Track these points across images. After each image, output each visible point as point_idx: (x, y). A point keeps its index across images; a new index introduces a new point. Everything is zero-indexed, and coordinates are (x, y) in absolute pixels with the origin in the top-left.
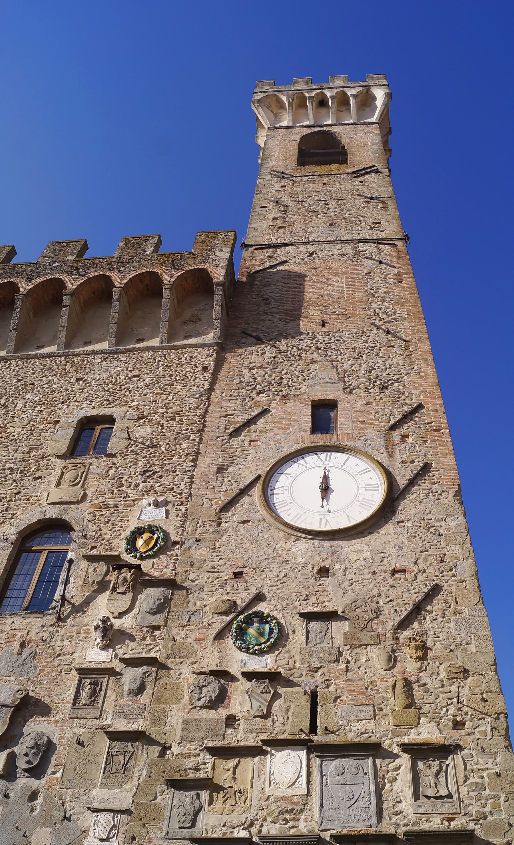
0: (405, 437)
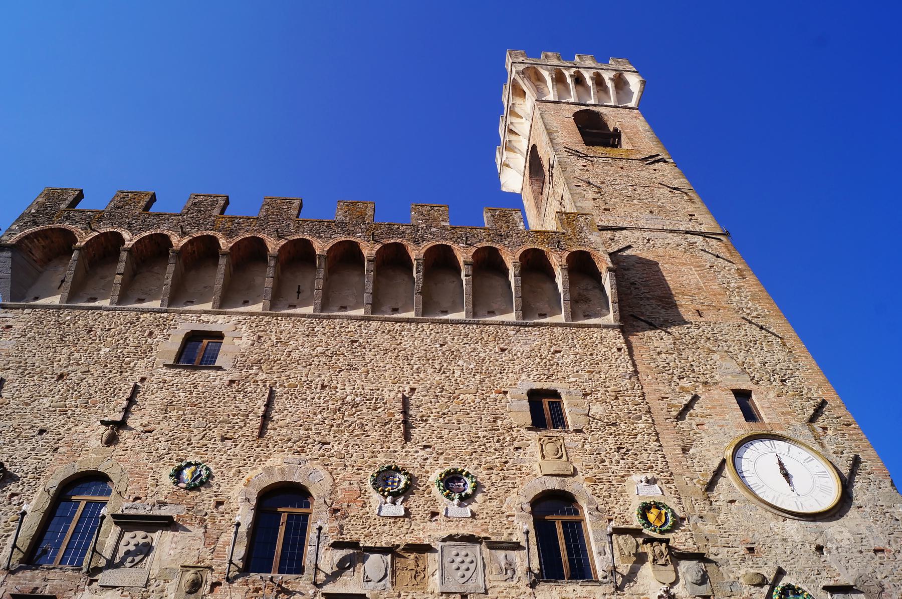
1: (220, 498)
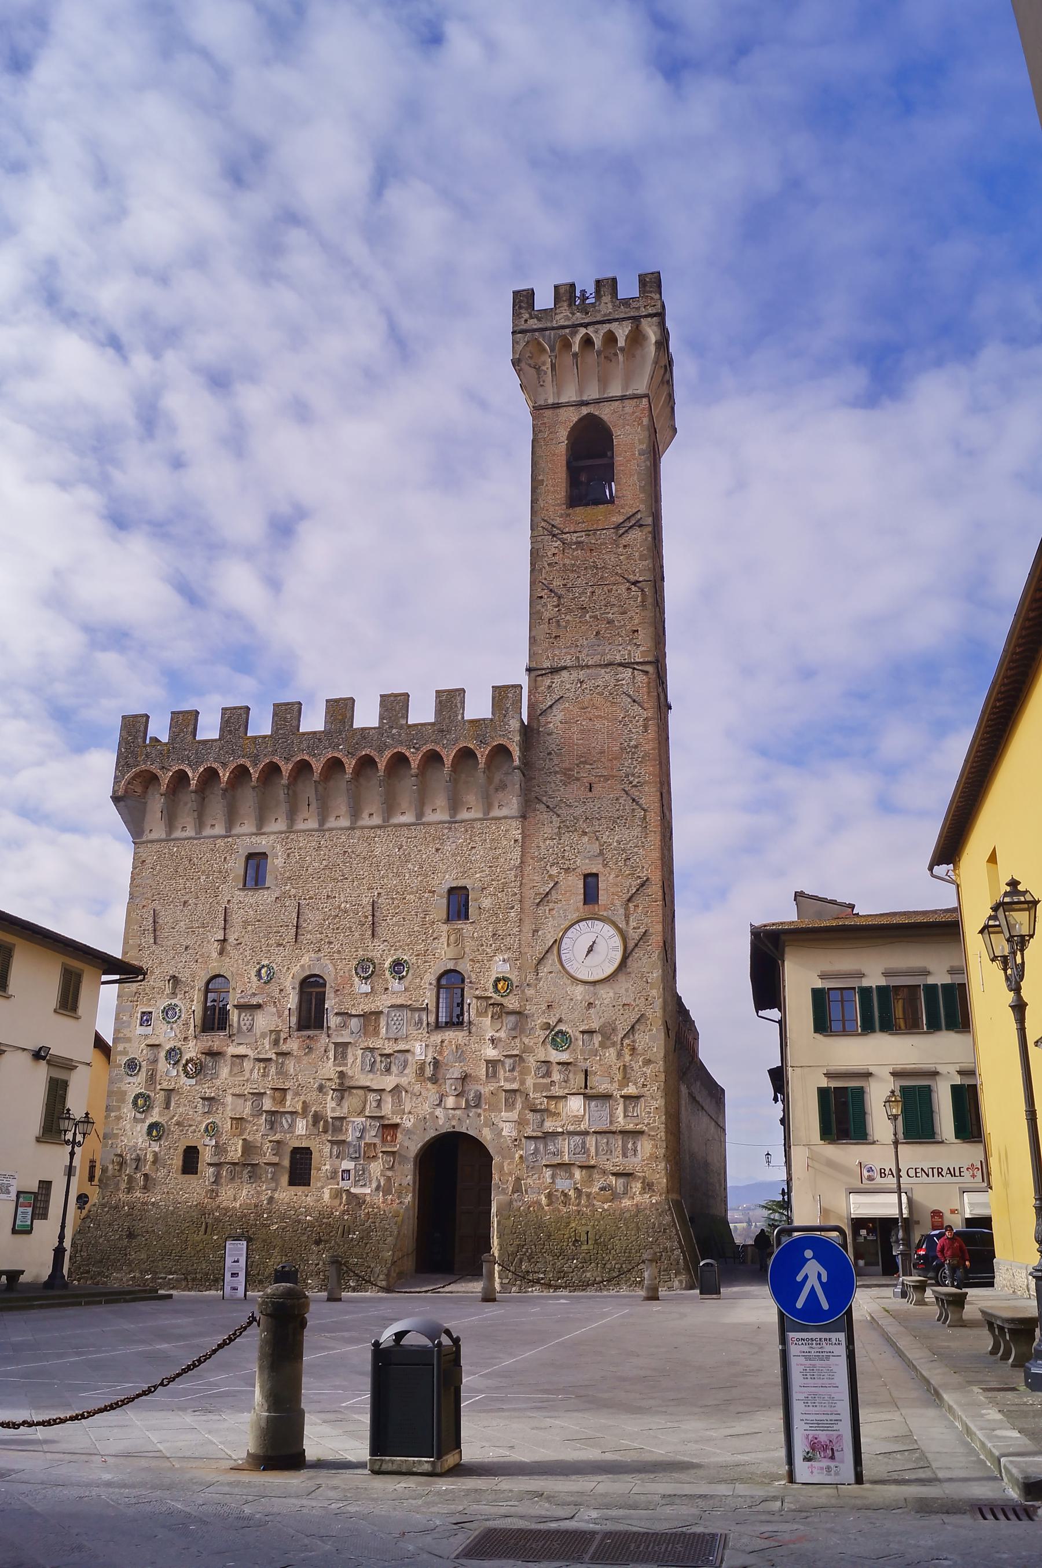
0: (637, 906)
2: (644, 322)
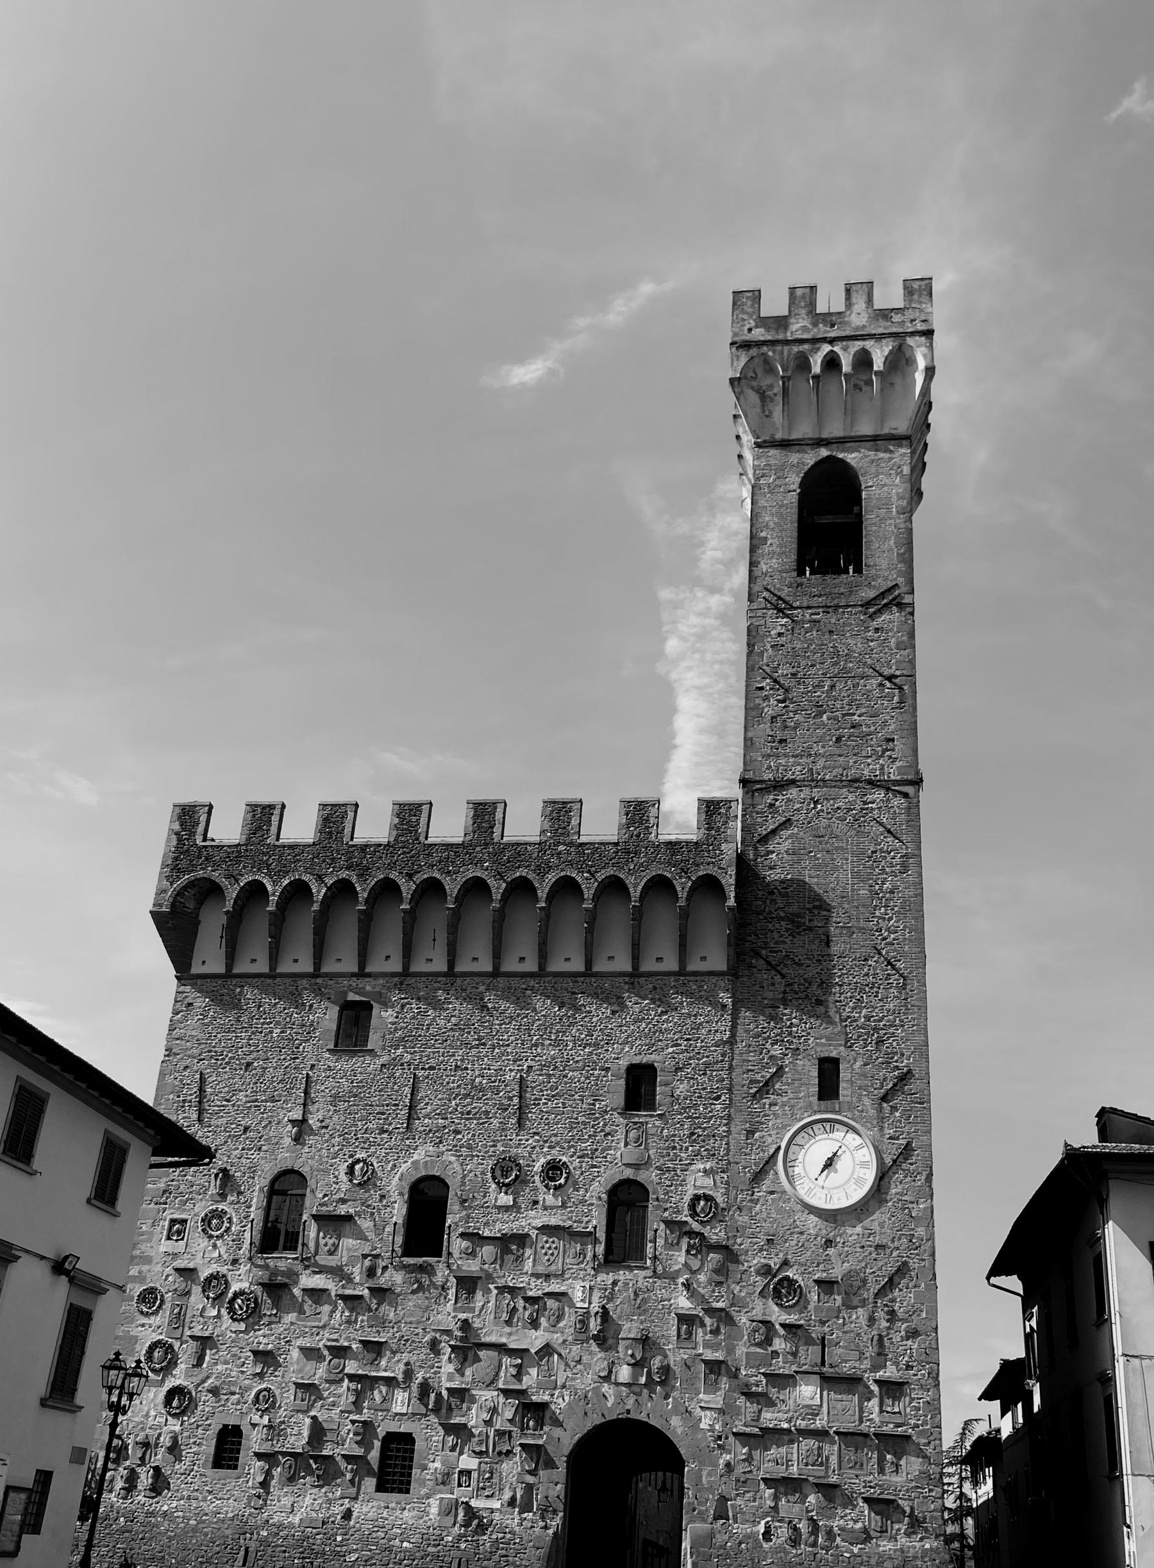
0: (894, 1109)
1: (384, 1192)
2: (910, 341)
